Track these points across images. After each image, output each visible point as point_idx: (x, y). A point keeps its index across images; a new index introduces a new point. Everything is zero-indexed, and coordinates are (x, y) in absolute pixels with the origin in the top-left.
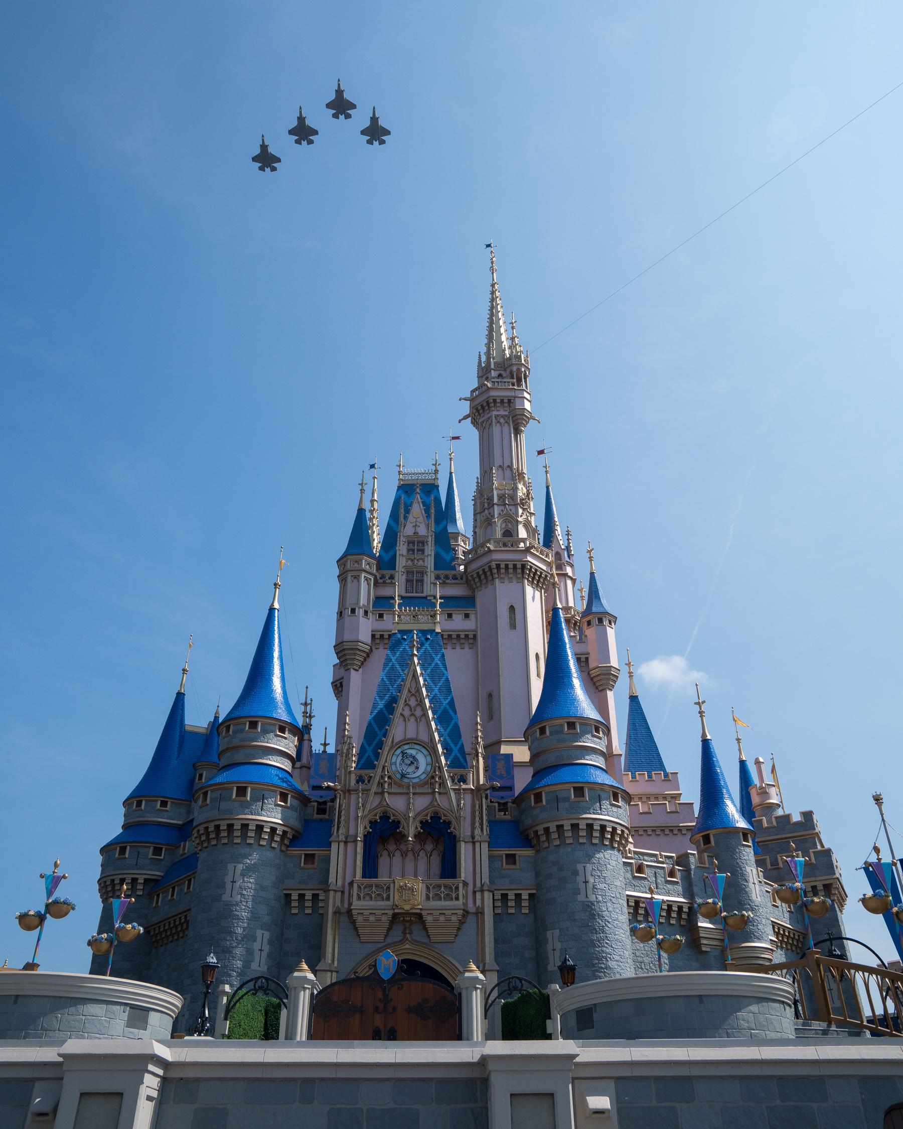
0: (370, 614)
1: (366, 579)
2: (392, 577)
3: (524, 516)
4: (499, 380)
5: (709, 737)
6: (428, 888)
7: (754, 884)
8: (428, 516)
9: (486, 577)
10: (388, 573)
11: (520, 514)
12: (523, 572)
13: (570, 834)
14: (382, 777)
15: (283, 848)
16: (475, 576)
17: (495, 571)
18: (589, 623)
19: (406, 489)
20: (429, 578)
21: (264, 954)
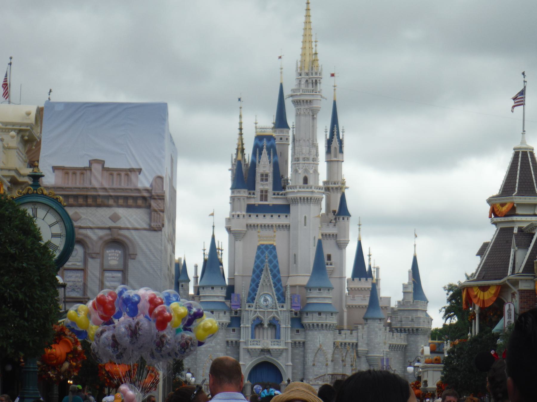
0: (245, 216)
1: (244, 199)
2: (254, 194)
3: (314, 168)
4: (306, 88)
7: (380, 336)
8: (270, 162)
10: (252, 192)
12: (310, 201)
13: (316, 327)
14: (256, 306)
15: (226, 328)
17: (299, 200)
18: (339, 219)
20: (270, 195)
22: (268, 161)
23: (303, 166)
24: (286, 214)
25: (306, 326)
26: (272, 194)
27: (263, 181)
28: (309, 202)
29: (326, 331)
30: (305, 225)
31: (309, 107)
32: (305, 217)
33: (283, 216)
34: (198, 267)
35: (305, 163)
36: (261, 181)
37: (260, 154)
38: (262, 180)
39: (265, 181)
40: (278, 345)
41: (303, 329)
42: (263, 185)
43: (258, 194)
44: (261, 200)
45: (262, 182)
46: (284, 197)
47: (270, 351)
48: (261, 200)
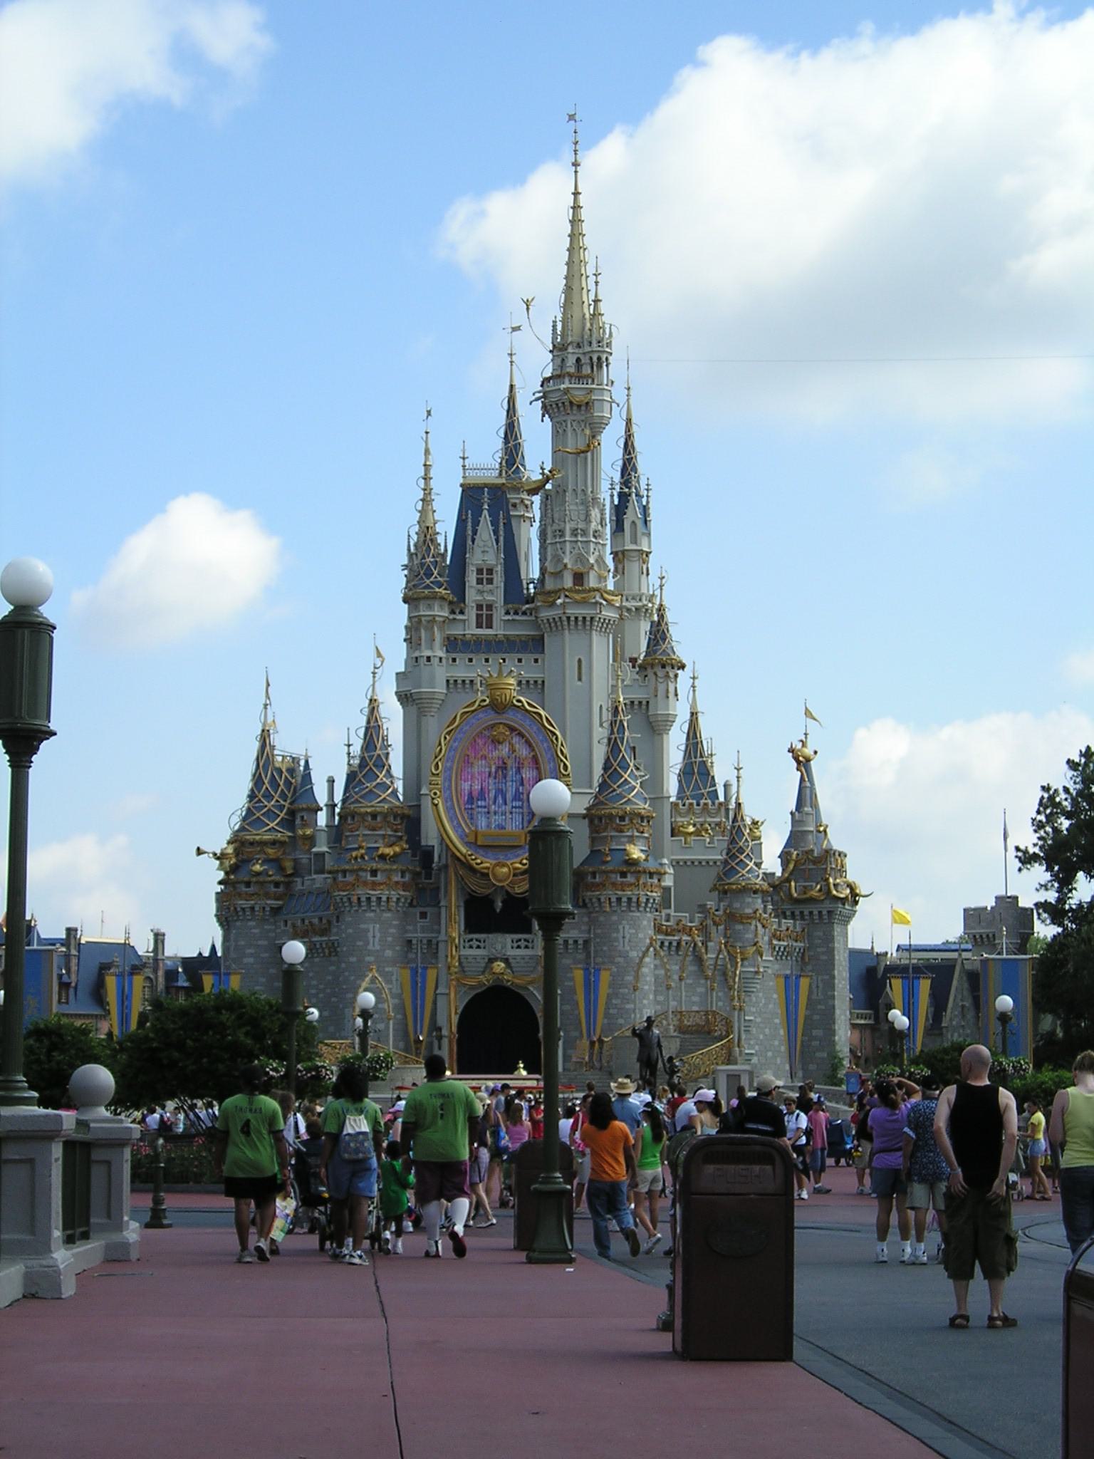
0: (444, 660)
3: (597, 553)
5: (741, 801)
6: (513, 941)
8: (497, 541)
9: (557, 627)
11: (592, 550)
15: (405, 909)
16: (545, 621)
17: (565, 623)
19: (472, 495)
20: (499, 615)
22: (493, 537)
24: (536, 656)
25: (592, 904)
26: (503, 612)
27: (482, 584)
28: (588, 628)
29: (638, 914)
30: (580, 679)
31: (583, 418)
32: (580, 661)
33: (528, 658)
34: (335, 784)
35: (577, 542)
36: (478, 583)
37: (476, 523)
38: (480, 581)
39: (487, 584)
40: (526, 947)
41: (584, 910)
42: (480, 592)
43: (471, 614)
44: (479, 626)
45: (480, 586)
46: (530, 618)
47: (511, 961)
48: (479, 626)
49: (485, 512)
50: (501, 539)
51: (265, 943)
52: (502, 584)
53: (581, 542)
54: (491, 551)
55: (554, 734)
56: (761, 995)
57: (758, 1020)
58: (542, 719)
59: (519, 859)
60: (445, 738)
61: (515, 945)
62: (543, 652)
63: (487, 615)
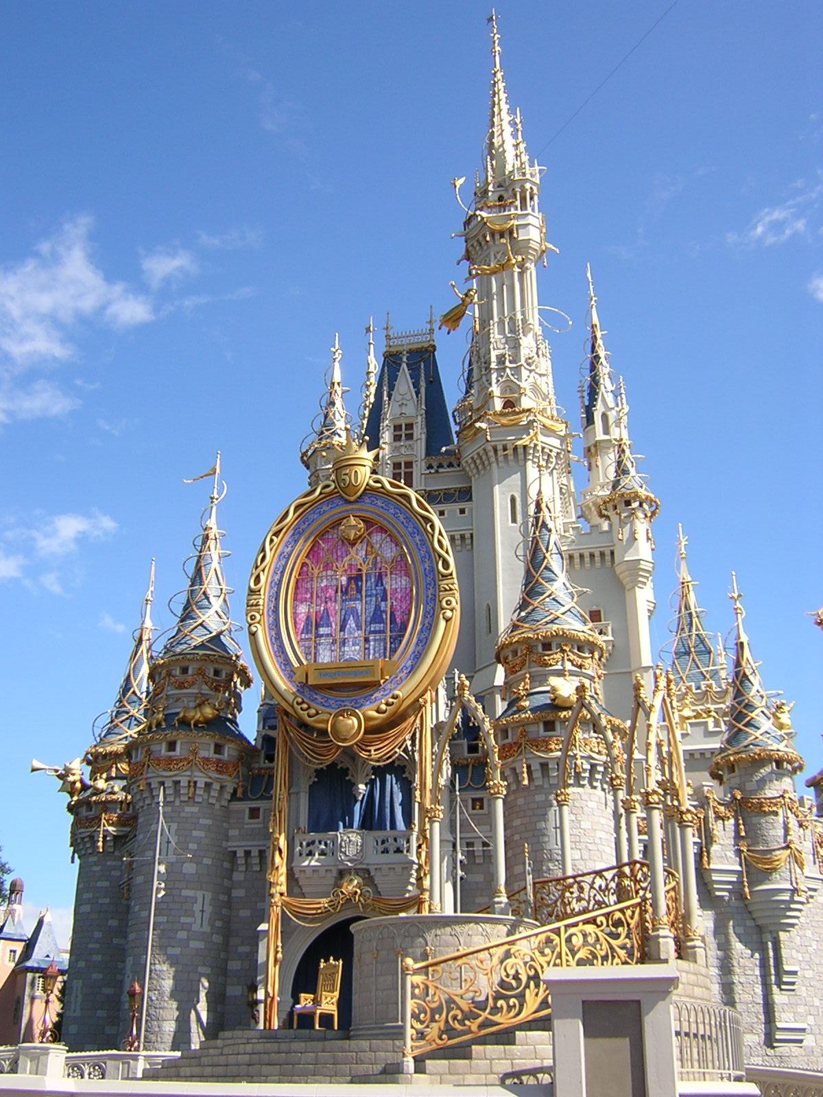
3: (531, 380)
8: (417, 393)
16: (470, 461)
17: (492, 454)
21: (207, 916)
22: (413, 390)
23: (502, 376)
24: (462, 505)
29: (580, 790)
38: (397, 438)
45: (397, 444)
49: (404, 365)
50: (423, 390)
51: (106, 884)
52: (424, 436)
53: (510, 368)
54: (410, 404)
55: (427, 520)
56: (809, 933)
57: (809, 974)
58: (410, 503)
59: (375, 705)
60: (272, 541)
61: (381, 848)
62: (470, 499)
63: (405, 473)
